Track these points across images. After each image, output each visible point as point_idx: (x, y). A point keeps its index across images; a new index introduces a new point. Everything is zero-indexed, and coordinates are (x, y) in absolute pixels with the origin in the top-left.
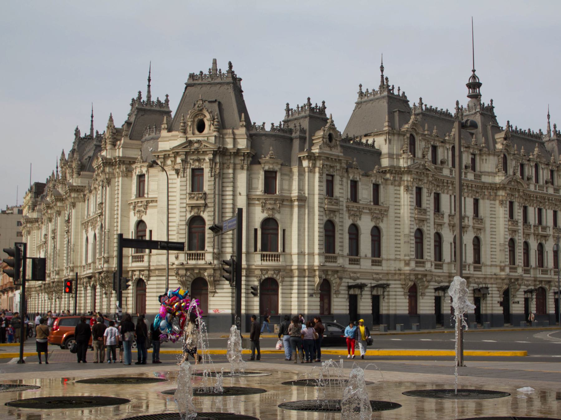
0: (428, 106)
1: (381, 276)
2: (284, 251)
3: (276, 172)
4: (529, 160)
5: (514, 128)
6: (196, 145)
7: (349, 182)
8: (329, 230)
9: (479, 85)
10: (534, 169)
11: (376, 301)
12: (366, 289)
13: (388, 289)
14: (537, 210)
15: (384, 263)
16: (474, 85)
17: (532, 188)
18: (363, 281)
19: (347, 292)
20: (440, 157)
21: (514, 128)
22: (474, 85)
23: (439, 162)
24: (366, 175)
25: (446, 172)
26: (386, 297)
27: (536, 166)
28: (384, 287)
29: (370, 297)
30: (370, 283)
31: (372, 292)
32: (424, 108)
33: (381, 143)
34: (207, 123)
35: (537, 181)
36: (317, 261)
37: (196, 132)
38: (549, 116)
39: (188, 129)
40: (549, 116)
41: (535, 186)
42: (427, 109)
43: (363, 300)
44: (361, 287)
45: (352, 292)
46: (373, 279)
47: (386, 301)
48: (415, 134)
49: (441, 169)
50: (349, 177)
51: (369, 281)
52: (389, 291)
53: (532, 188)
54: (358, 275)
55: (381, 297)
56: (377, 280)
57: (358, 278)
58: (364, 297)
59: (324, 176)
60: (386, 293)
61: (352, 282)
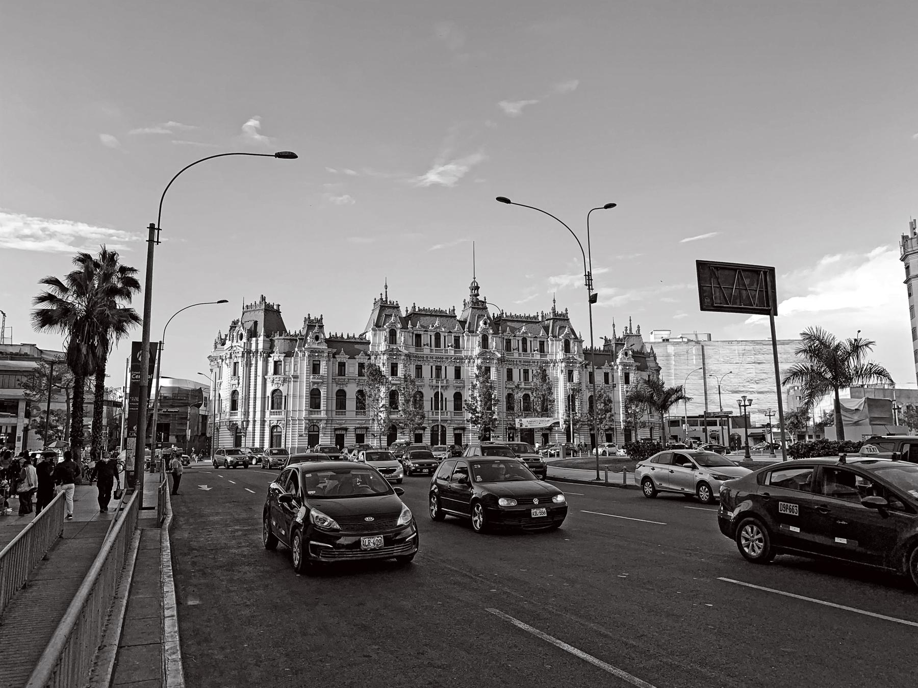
0: (421, 308)
21: (508, 314)
24: (352, 357)
25: (426, 350)
28: (367, 428)
30: (351, 427)
33: (369, 336)
36: (304, 414)
42: (419, 310)
44: (346, 429)
61: (337, 426)
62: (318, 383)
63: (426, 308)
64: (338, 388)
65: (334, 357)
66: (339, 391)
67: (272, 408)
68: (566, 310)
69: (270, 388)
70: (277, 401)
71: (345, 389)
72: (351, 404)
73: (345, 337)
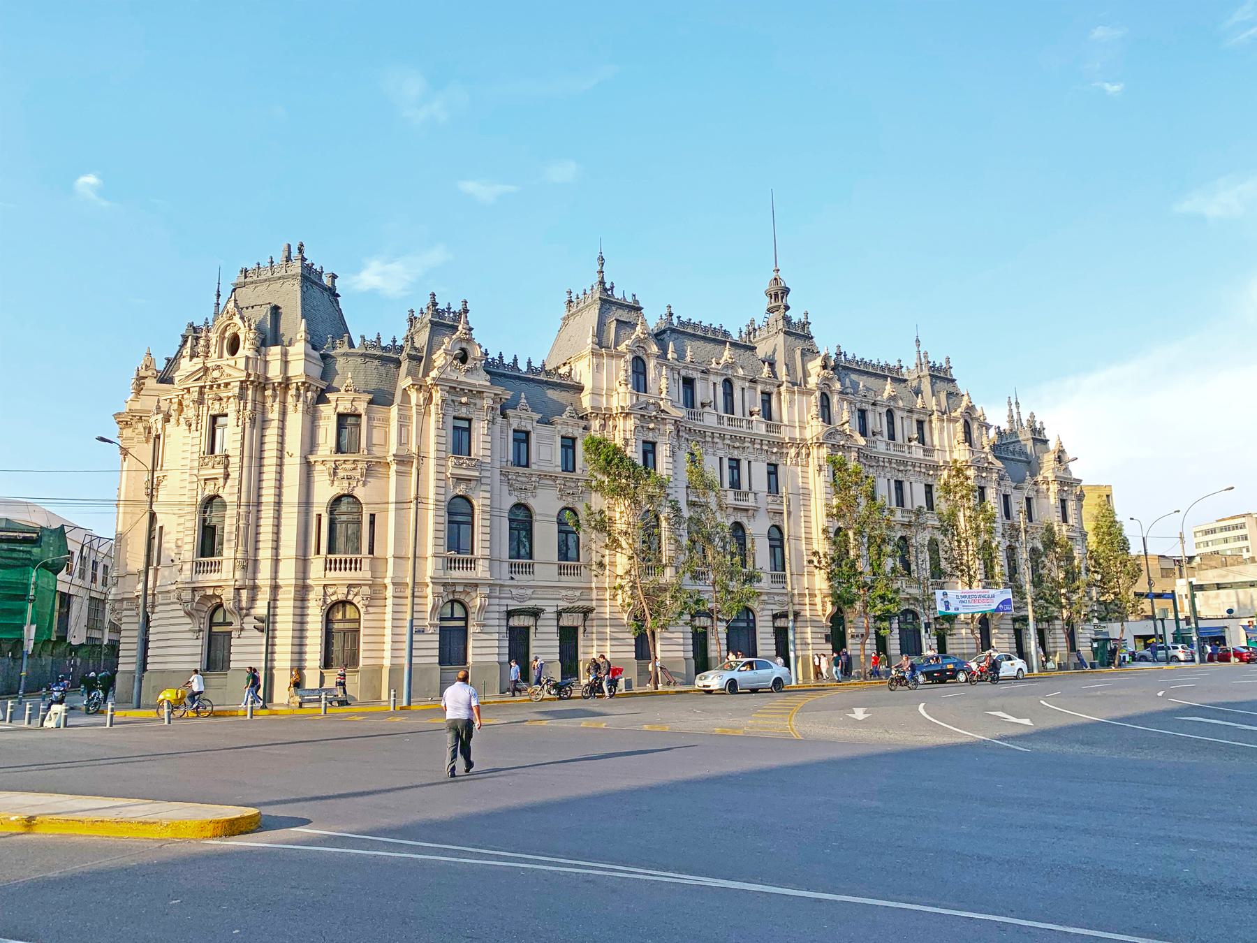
0: (684, 319)
2: (371, 551)
3: (359, 416)
4: (874, 404)
5: (849, 357)
6: (216, 374)
7: (511, 433)
8: (458, 515)
9: (786, 291)
10: (885, 419)
11: (568, 638)
14: (892, 482)
16: (780, 293)
17: (881, 447)
18: (539, 603)
19: (504, 623)
20: (699, 398)
22: (780, 293)
23: (699, 405)
24: (546, 421)
25: (710, 420)
27: (890, 413)
28: (586, 612)
29: (555, 629)
31: (558, 620)
32: (675, 322)
33: (583, 372)
34: (242, 338)
35: (892, 436)
36: (430, 568)
37: (226, 354)
38: (918, 341)
39: (212, 349)
40: (918, 341)
41: (888, 444)
42: (682, 323)
44: (536, 613)
45: (516, 622)
48: (644, 357)
49: (701, 414)
50: (509, 424)
51: (555, 603)
53: (881, 447)
59: (450, 420)
61: (514, 605)
62: (468, 480)
63: (695, 320)
64: (513, 500)
65: (504, 416)
66: (518, 506)
67: (331, 550)
68: (948, 360)
69: (324, 492)
70: (345, 529)
71: (531, 502)
72: (545, 538)
73: (523, 366)
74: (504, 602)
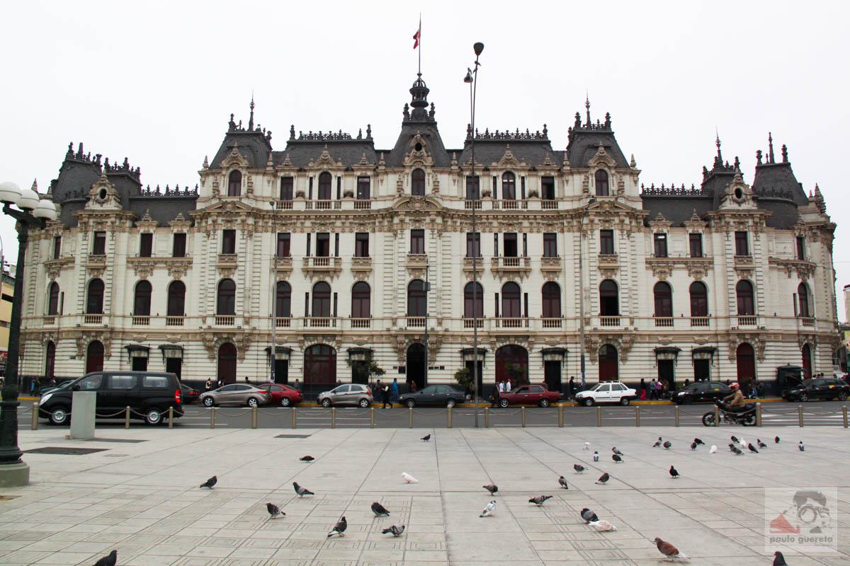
1: (706, 338)
12: (680, 353)
13: (715, 353)
15: (712, 322)
18: (678, 345)
19: (654, 358)
26: (715, 362)
28: (712, 351)
31: (692, 356)
43: (679, 367)
46: (695, 342)
47: (717, 366)
51: (690, 345)
52: (718, 355)
54: (670, 338)
55: (710, 362)
56: (701, 343)
57: (671, 342)
58: (679, 362)
60: (714, 358)
74: (654, 345)
